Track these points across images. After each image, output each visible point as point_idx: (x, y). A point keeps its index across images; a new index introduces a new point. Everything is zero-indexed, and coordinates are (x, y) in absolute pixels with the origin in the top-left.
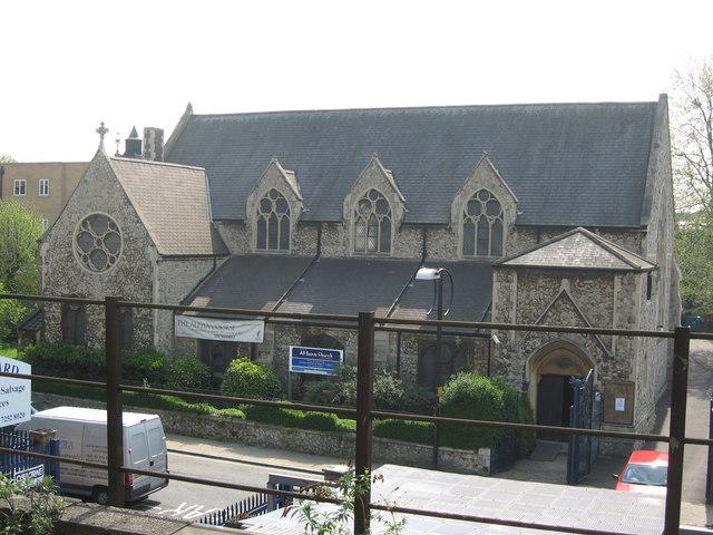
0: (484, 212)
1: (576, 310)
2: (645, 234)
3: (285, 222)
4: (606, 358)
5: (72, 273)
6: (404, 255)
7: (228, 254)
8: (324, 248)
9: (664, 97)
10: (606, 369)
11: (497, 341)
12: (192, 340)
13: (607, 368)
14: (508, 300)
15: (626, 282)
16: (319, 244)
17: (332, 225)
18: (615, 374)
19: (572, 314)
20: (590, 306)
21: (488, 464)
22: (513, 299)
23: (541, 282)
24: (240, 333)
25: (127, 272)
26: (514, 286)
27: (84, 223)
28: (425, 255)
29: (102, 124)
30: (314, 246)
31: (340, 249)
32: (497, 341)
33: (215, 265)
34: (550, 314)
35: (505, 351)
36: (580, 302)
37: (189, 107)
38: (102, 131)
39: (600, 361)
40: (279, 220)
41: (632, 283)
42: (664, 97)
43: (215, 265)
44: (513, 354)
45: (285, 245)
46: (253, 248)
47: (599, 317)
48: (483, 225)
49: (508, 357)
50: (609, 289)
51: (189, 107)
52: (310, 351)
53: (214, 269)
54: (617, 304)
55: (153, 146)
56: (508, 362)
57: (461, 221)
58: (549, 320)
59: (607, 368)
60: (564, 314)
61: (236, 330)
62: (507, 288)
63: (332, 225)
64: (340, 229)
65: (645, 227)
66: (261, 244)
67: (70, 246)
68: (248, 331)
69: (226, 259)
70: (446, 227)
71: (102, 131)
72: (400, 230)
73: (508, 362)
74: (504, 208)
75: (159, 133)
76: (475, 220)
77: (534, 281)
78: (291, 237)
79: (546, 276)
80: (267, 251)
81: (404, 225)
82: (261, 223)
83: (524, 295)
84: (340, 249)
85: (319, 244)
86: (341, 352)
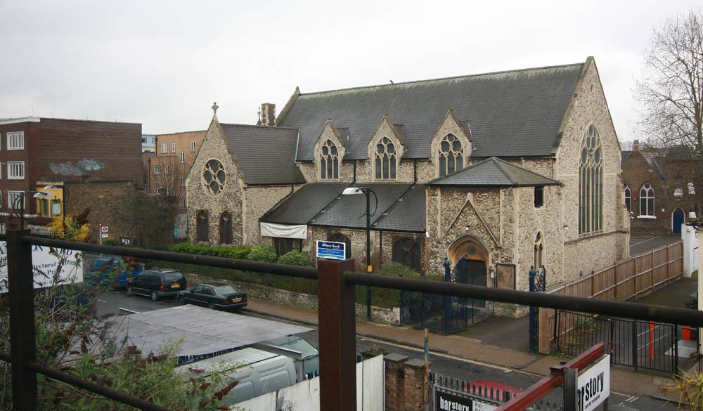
0: (386, 151)
2: (555, 159)
3: (336, 160)
4: (497, 248)
5: (201, 197)
6: (403, 181)
9: (591, 59)
10: (497, 255)
11: (428, 236)
12: (269, 237)
13: (498, 254)
14: (435, 208)
15: (507, 193)
16: (355, 175)
17: (362, 161)
19: (474, 217)
21: (398, 318)
22: (439, 207)
24: (294, 233)
25: (229, 195)
26: (439, 198)
27: (207, 166)
28: (416, 179)
29: (215, 103)
30: (352, 176)
31: (367, 178)
32: (428, 236)
33: (293, 189)
34: (461, 217)
35: (435, 243)
36: (479, 208)
38: (215, 108)
39: (493, 249)
40: (333, 159)
42: (591, 59)
43: (293, 189)
44: (440, 245)
45: (336, 176)
46: (319, 179)
47: (492, 219)
48: (451, 156)
49: (437, 247)
50: (497, 199)
51: (298, 88)
52: (328, 244)
53: (291, 193)
54: (502, 209)
55: (267, 116)
56: (437, 250)
57: (438, 156)
59: (498, 254)
60: (469, 217)
61: (293, 231)
62: (435, 200)
63: (362, 161)
65: (554, 155)
66: (323, 176)
67: (200, 178)
68: (298, 231)
69: (302, 185)
70: (427, 160)
71: (215, 108)
72: (401, 163)
73: (437, 250)
74: (463, 146)
75: (272, 107)
76: (446, 154)
79: (473, 192)
80: (327, 180)
81: (404, 160)
82: (323, 161)
83: (445, 204)
84: (367, 178)
85: (355, 175)
86: (344, 244)
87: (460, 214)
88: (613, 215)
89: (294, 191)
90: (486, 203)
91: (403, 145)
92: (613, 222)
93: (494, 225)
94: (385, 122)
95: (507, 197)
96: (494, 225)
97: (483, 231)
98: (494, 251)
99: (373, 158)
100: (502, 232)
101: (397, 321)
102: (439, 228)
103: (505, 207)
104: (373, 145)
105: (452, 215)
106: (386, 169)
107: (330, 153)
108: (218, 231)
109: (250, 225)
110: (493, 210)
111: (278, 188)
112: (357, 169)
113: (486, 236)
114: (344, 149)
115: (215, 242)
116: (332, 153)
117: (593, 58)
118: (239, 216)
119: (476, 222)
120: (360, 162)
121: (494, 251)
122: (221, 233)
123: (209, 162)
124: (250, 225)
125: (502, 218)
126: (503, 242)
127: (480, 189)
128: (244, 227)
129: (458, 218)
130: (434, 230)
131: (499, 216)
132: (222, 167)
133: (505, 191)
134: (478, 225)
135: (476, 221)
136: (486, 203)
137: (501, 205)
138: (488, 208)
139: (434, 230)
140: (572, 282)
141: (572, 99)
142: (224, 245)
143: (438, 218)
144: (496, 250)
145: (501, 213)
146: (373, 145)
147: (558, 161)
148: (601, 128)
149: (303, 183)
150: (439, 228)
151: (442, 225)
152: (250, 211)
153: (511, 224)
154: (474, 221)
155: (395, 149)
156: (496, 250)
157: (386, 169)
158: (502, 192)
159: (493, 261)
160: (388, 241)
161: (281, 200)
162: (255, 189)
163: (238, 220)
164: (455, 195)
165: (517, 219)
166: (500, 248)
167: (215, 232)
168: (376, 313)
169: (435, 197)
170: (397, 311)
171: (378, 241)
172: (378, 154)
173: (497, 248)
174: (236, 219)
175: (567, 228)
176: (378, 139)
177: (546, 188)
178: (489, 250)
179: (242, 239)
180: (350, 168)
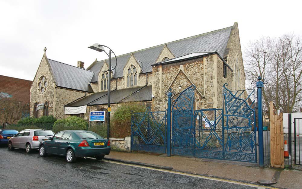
5: (36, 96)
7: (93, 92)
8: (118, 87)
10: (201, 104)
13: (202, 103)
14: (158, 79)
15: (209, 60)
16: (117, 86)
17: (120, 78)
18: (206, 106)
19: (185, 80)
20: (193, 75)
21: (129, 146)
22: (160, 78)
23: (172, 69)
24: (80, 110)
26: (160, 72)
28: (147, 84)
29: (45, 47)
30: (115, 86)
33: (86, 95)
34: (175, 82)
35: (158, 102)
36: (188, 74)
38: (45, 50)
39: (198, 100)
40: (107, 80)
41: (211, 59)
42: (236, 24)
43: (86, 95)
44: (161, 103)
46: (100, 90)
47: (197, 80)
49: (159, 104)
50: (201, 65)
51: (96, 59)
52: (95, 113)
53: (85, 96)
56: (159, 106)
58: (175, 84)
59: (202, 103)
60: (181, 81)
61: (79, 109)
62: (158, 74)
63: (120, 78)
64: (122, 79)
66: (102, 89)
67: (36, 87)
68: (82, 109)
69: (91, 94)
71: (45, 50)
73: (159, 106)
77: (169, 69)
80: (103, 90)
81: (141, 74)
82: (102, 82)
83: (165, 76)
84: (122, 86)
85: (117, 86)
86: (104, 112)
87: (175, 80)
90: (193, 70)
91: (141, 67)
95: (208, 62)
96: (198, 83)
98: (199, 101)
100: (205, 87)
101: (128, 148)
102: (160, 92)
103: (207, 69)
105: (169, 82)
111: (77, 92)
112: (118, 83)
118: (52, 103)
120: (119, 79)
123: (40, 78)
125: (205, 77)
126: (206, 93)
127: (189, 61)
128: (54, 109)
130: (157, 93)
131: (203, 77)
135: (186, 82)
136: (193, 70)
138: (195, 73)
139: (157, 93)
143: (160, 85)
144: (201, 100)
145: (204, 74)
150: (160, 92)
153: (211, 80)
154: (184, 83)
156: (201, 100)
158: (205, 59)
161: (79, 99)
163: (51, 105)
164: (172, 69)
168: (113, 143)
169: (158, 72)
173: (202, 98)
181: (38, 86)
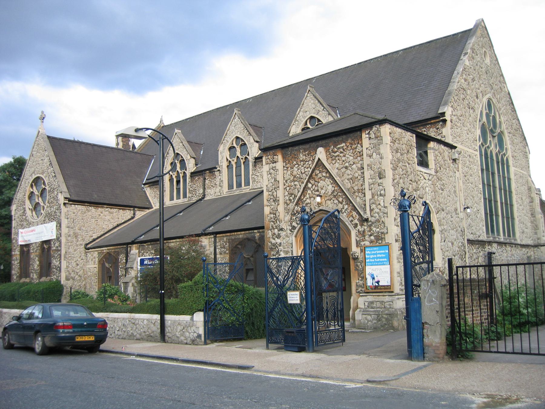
1: (331, 177)
2: (445, 121)
8: (208, 191)
13: (364, 231)
14: (275, 180)
15: (373, 136)
18: (372, 238)
19: (328, 181)
20: (344, 170)
21: (201, 331)
22: (280, 178)
23: (302, 157)
26: (280, 165)
30: (201, 191)
31: (218, 190)
33: (134, 214)
34: (310, 185)
35: (276, 231)
36: (333, 168)
37: (161, 121)
43: (134, 214)
45: (185, 196)
50: (359, 148)
53: (133, 218)
56: (278, 241)
58: (309, 192)
59: (364, 231)
60: (321, 183)
62: (274, 168)
63: (212, 170)
64: (217, 173)
65: (443, 114)
67: (24, 202)
69: (148, 211)
73: (278, 241)
77: (296, 158)
78: (188, 187)
83: (289, 172)
84: (218, 190)
87: (308, 181)
88: (527, 220)
89: (137, 217)
90: (344, 159)
91: (257, 142)
92: (529, 231)
93: (356, 188)
94: (237, 118)
95: (372, 141)
96: (356, 188)
97: (341, 199)
98: (359, 227)
99: (225, 164)
100: (368, 196)
101: (199, 336)
102: (281, 208)
103: (370, 156)
104: (224, 149)
105: (299, 186)
106: (239, 175)
107: (178, 169)
108: (38, 263)
109: (71, 250)
110: (354, 166)
111: (112, 210)
112: (207, 181)
113: (346, 207)
114: (193, 161)
115: (35, 276)
116: (181, 169)
117: (483, 20)
119: (330, 188)
120: (210, 172)
121: (359, 227)
122: (41, 265)
123: (33, 182)
124: (71, 250)
125: (367, 174)
126: (371, 210)
127: (335, 139)
128: (63, 252)
129: (305, 188)
131: (363, 173)
132: (44, 184)
133: (369, 133)
134: (333, 192)
135: (330, 186)
136: (344, 159)
137: (365, 155)
138: (347, 164)
139: (274, 212)
140: (490, 47)
141: (462, 57)
142: (44, 279)
144: (362, 225)
145: (365, 167)
146: (224, 149)
147: (448, 123)
148: (500, 106)
149: (148, 208)
150: (281, 208)
151: (285, 203)
152: (71, 233)
153: (380, 181)
154: (327, 186)
155: (249, 149)
156: (362, 225)
157: (239, 175)
158: (364, 136)
159: (358, 244)
160: (224, 247)
161: (118, 226)
162: (79, 207)
164: (302, 157)
165: (389, 174)
166: (367, 220)
167: (35, 264)
169: (274, 165)
170: (199, 317)
171: (212, 249)
172: (229, 159)
174: (54, 244)
175: (468, 210)
176: (229, 140)
177: (432, 144)
178: (351, 227)
179: (60, 268)
180: (199, 181)
181: (27, 202)
